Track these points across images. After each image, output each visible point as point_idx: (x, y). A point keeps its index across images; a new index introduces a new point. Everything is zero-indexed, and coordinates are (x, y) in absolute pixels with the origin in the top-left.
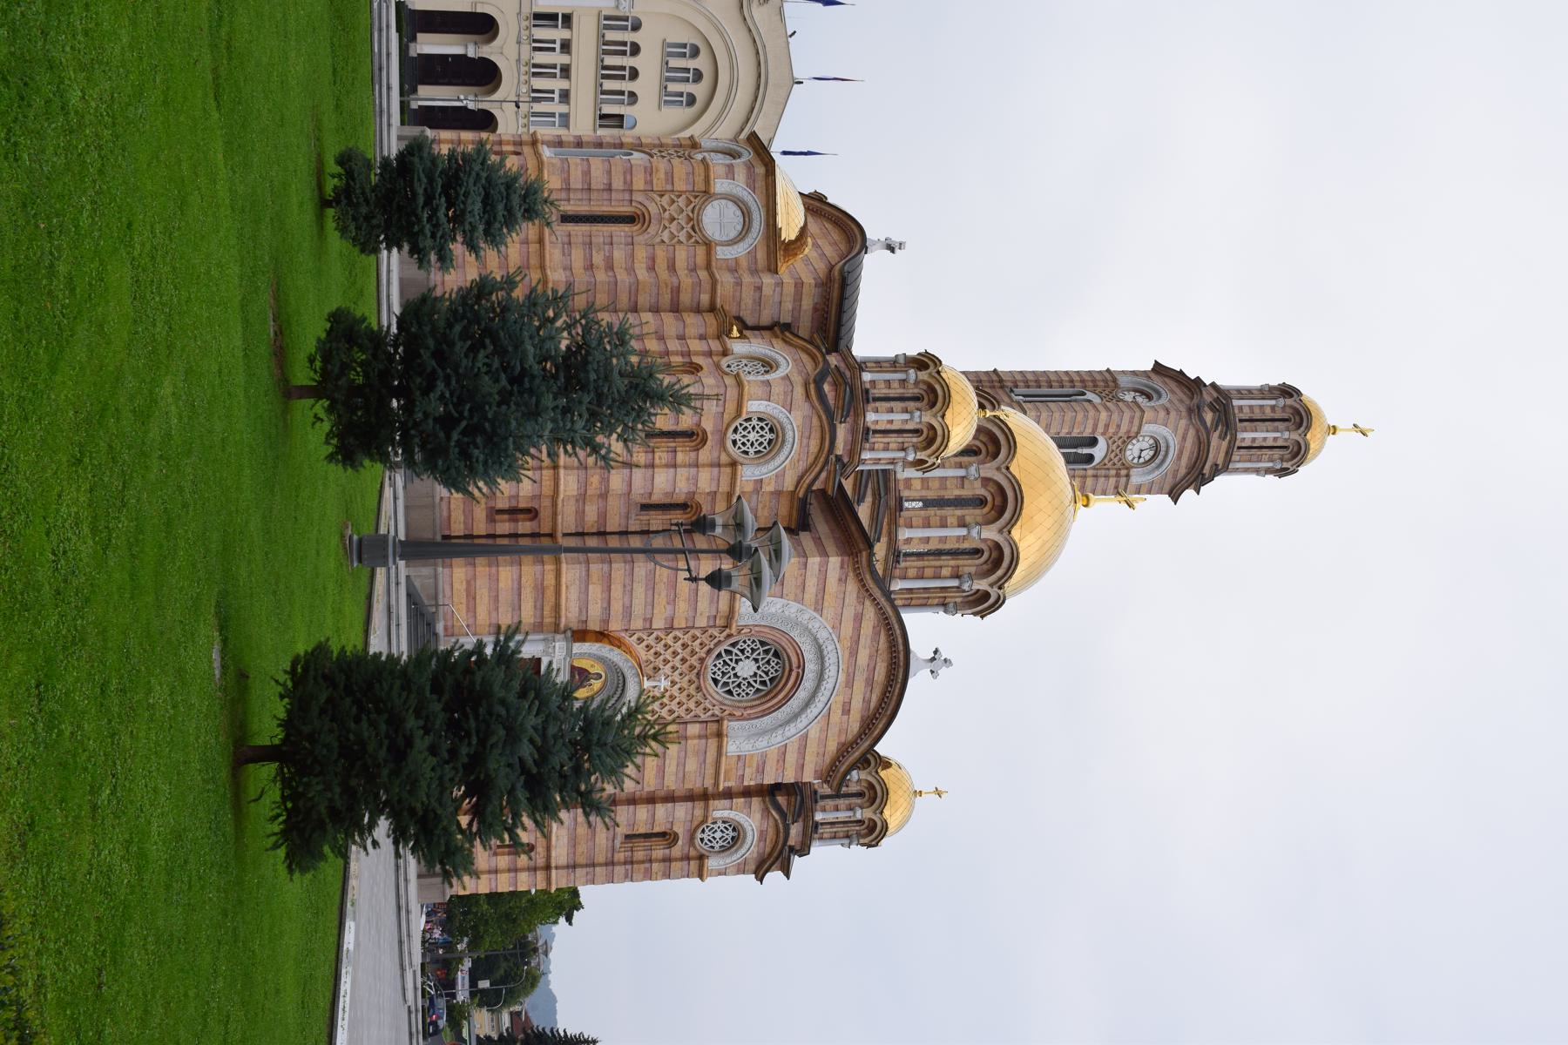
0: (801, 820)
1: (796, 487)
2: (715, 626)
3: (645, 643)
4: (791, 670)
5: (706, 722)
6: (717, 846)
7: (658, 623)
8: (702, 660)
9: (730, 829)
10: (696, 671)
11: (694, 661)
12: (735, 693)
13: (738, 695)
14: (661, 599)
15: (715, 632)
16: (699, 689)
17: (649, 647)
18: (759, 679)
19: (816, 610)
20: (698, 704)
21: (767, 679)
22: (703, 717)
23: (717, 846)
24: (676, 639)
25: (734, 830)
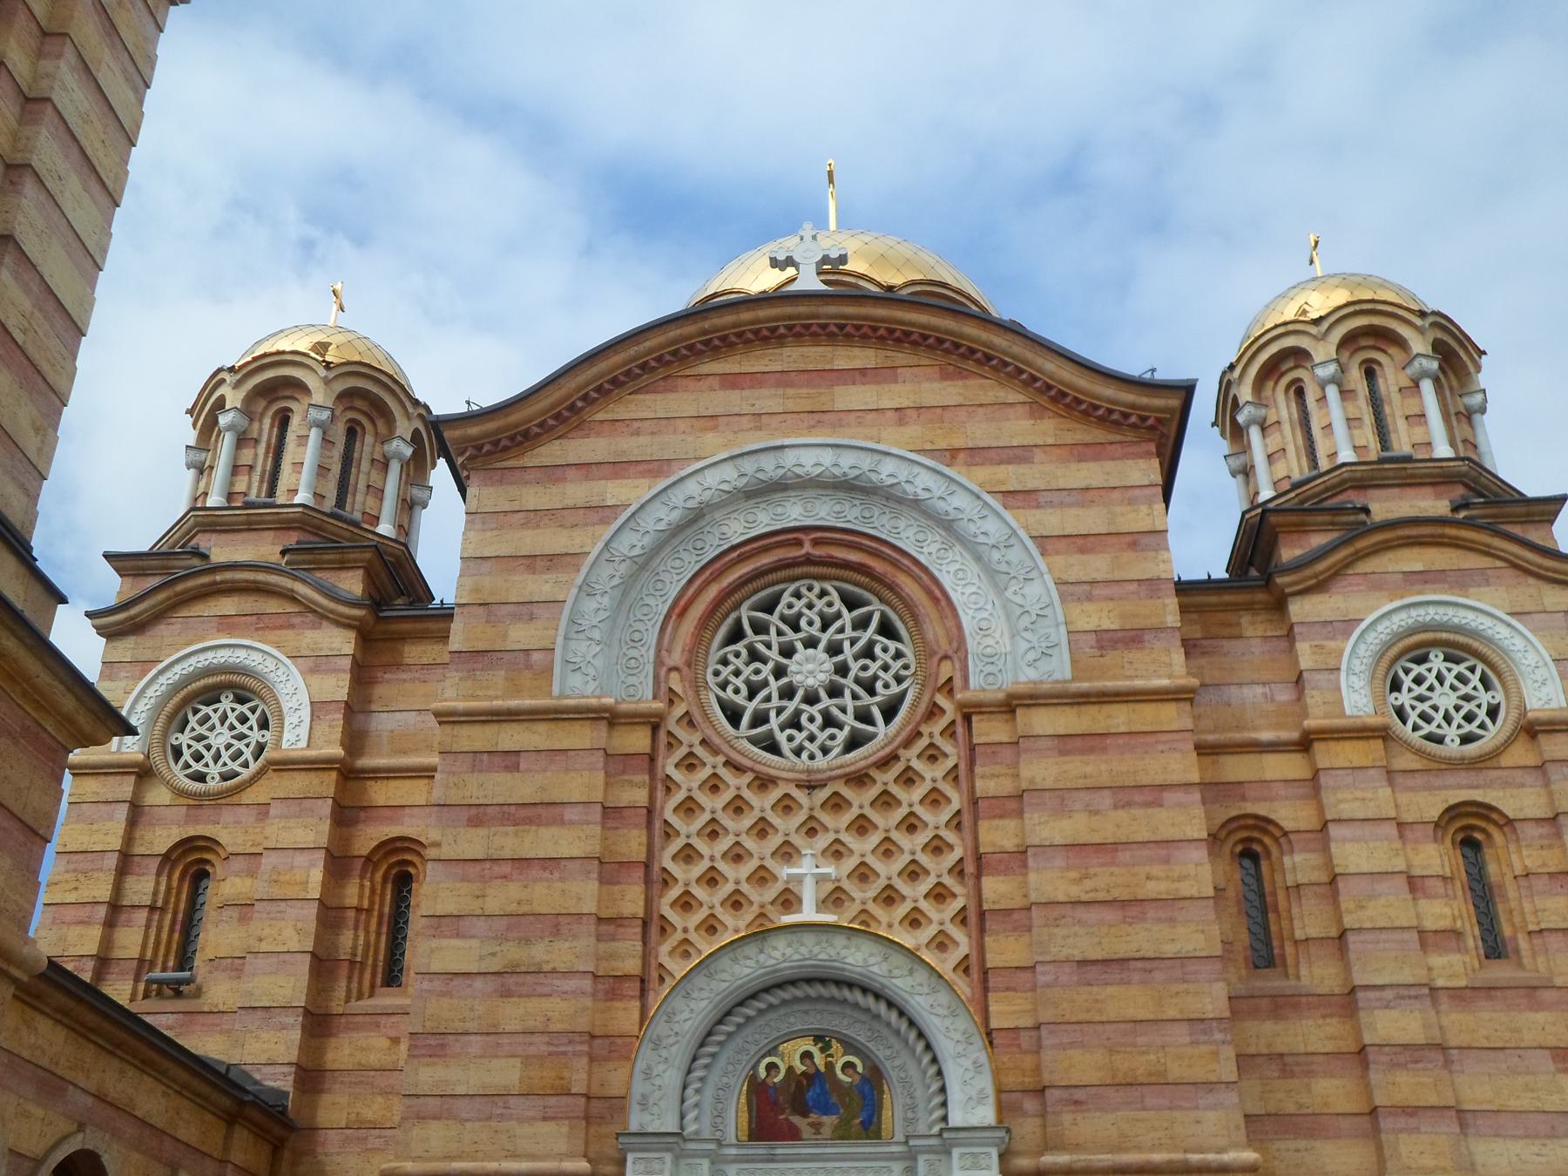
1: (348, 626)
2: (652, 759)
4: (809, 560)
5: (972, 748)
6: (1485, 698)
8: (764, 782)
9: (1421, 669)
11: (761, 803)
12: (895, 689)
13: (899, 680)
16: (859, 779)
19: (605, 522)
20: (909, 778)
22: (953, 753)
24: (688, 854)
25: (1421, 660)
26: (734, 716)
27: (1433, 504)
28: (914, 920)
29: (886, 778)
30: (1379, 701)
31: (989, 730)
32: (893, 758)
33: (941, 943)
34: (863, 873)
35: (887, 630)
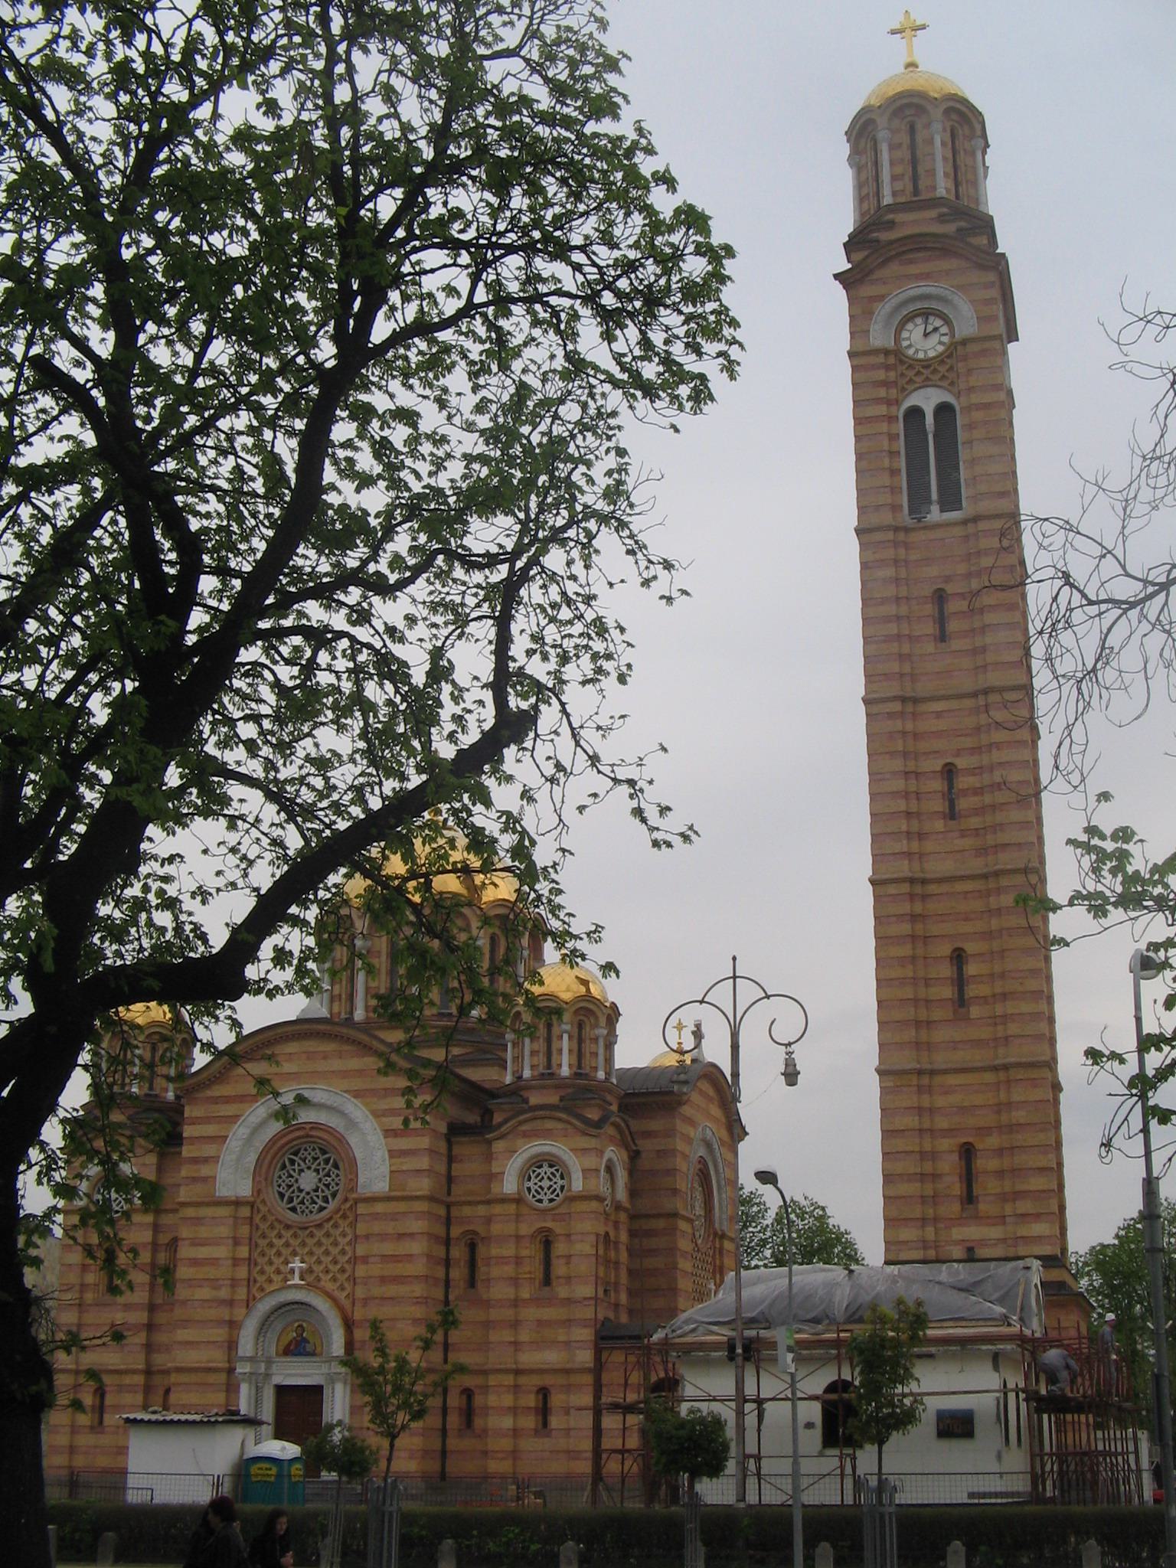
0: (525, 1094)
2: (251, 1218)
3: (265, 1286)
6: (560, 1182)
7: (242, 1272)
8: (288, 1227)
10: (299, 1232)
14: (211, 1272)
15: (257, 1219)
16: (319, 1226)
17: (270, 1281)
18: (322, 1166)
20: (335, 1226)
21: (322, 1158)
23: (560, 1182)
25: (540, 1167)
26: (282, 1195)
27: (553, 1098)
28: (334, 1279)
29: (328, 1226)
30: (521, 1183)
31: (362, 1209)
32: (330, 1219)
33: (342, 1288)
34: (319, 1262)
35: (336, 1166)
